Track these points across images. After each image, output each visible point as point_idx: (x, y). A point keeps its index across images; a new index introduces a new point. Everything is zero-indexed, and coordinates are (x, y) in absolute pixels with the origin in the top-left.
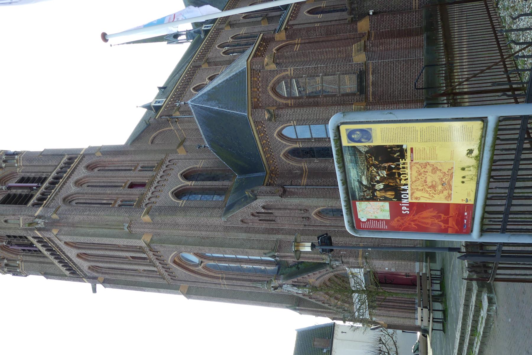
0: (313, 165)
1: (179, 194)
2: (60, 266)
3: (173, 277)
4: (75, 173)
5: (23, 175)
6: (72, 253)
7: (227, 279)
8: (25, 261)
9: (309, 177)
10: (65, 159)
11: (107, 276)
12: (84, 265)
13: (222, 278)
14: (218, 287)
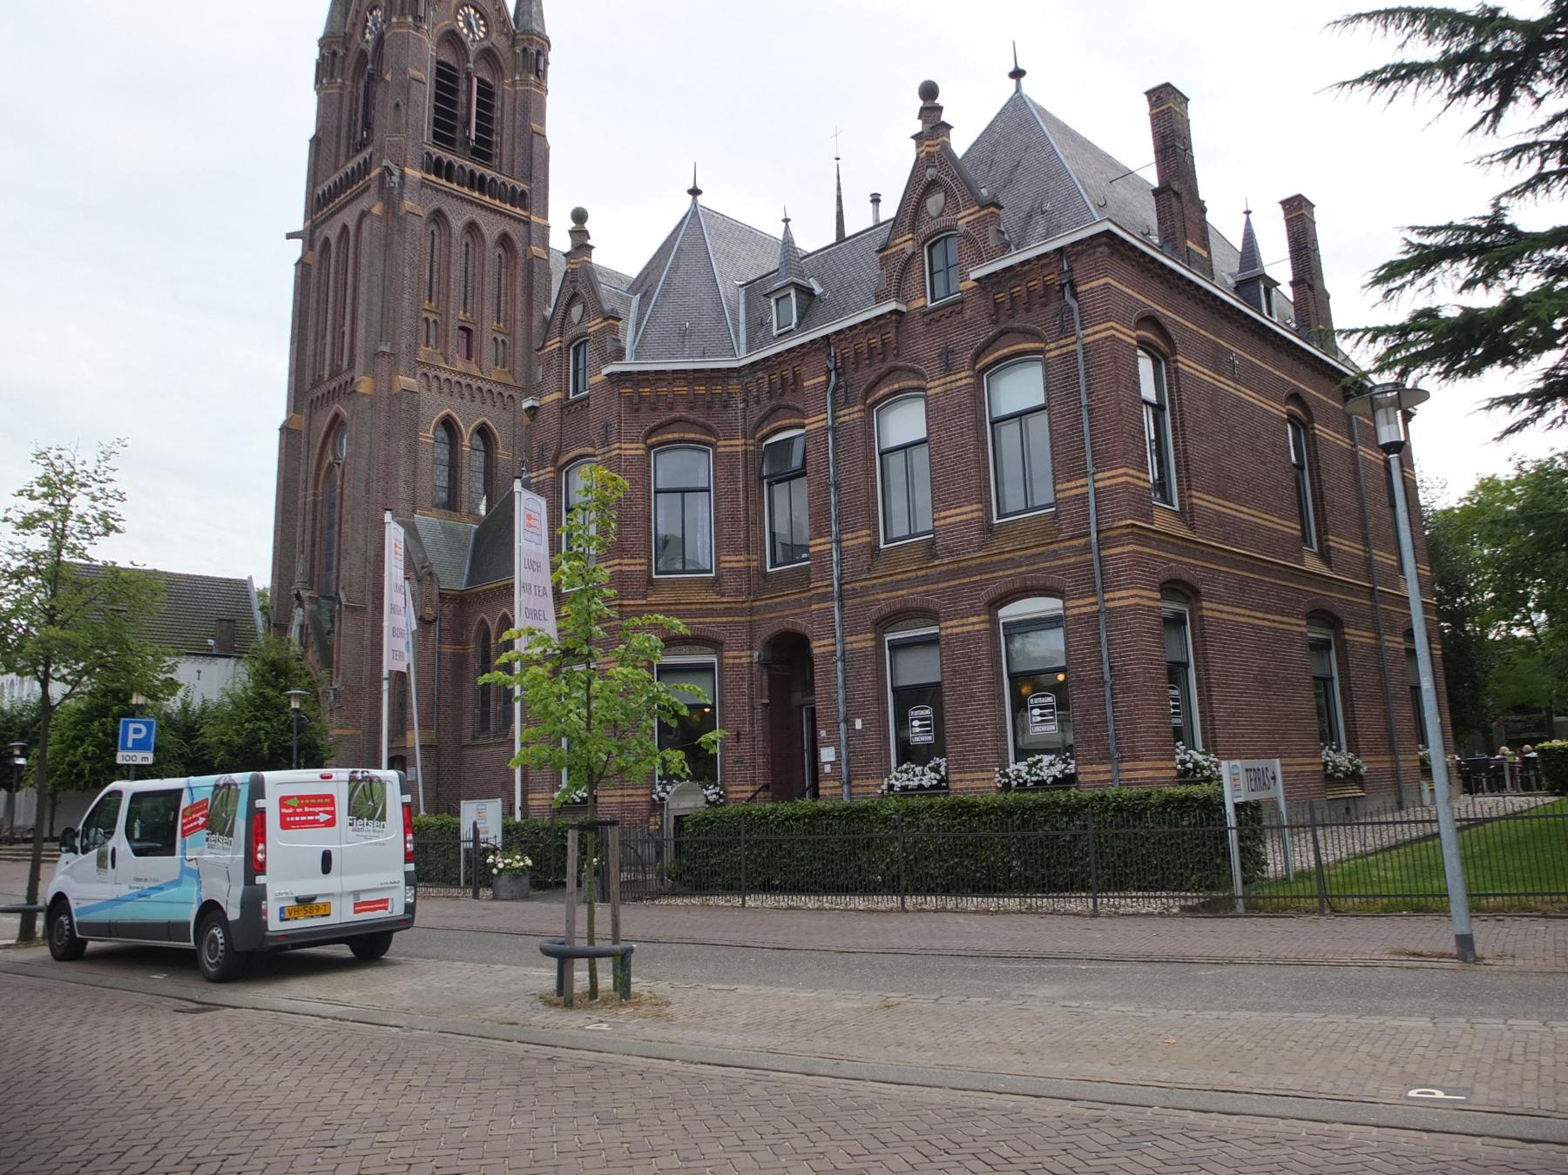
0: (471, 660)
1: (448, 424)
2: (330, 182)
3: (316, 404)
4: (492, 216)
5: (498, 91)
6: (349, 217)
7: (315, 503)
8: (341, 96)
9: (454, 654)
10: (521, 186)
11: (315, 270)
12: (332, 232)
13: (315, 495)
14: (301, 486)
